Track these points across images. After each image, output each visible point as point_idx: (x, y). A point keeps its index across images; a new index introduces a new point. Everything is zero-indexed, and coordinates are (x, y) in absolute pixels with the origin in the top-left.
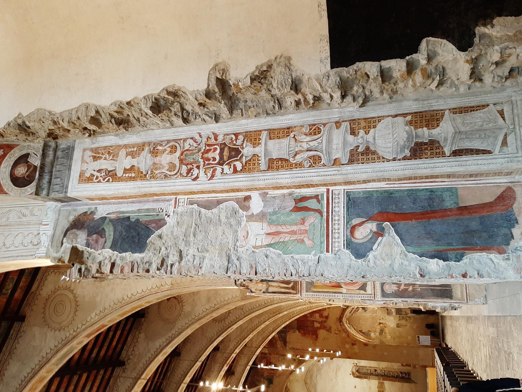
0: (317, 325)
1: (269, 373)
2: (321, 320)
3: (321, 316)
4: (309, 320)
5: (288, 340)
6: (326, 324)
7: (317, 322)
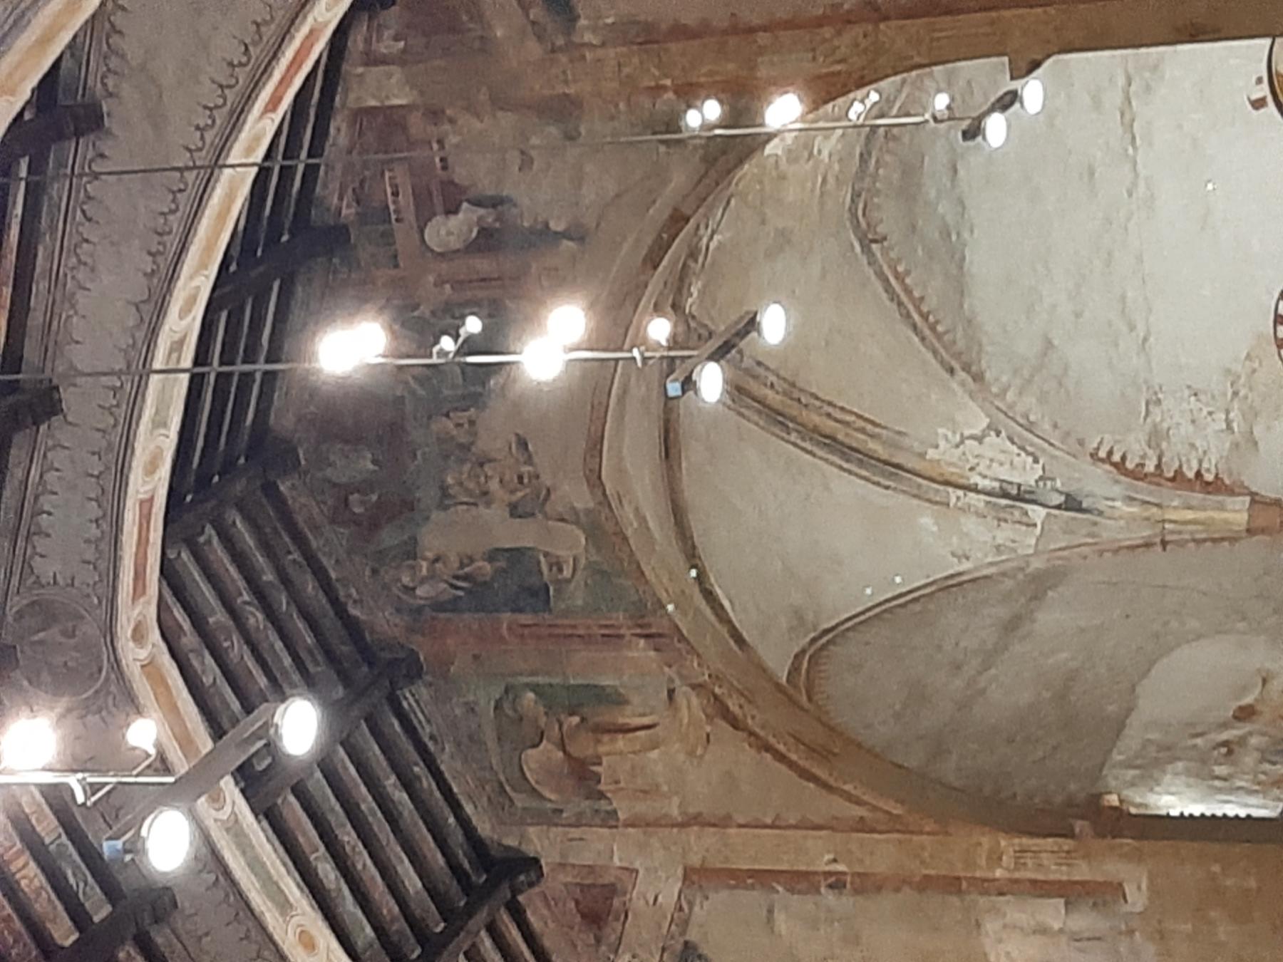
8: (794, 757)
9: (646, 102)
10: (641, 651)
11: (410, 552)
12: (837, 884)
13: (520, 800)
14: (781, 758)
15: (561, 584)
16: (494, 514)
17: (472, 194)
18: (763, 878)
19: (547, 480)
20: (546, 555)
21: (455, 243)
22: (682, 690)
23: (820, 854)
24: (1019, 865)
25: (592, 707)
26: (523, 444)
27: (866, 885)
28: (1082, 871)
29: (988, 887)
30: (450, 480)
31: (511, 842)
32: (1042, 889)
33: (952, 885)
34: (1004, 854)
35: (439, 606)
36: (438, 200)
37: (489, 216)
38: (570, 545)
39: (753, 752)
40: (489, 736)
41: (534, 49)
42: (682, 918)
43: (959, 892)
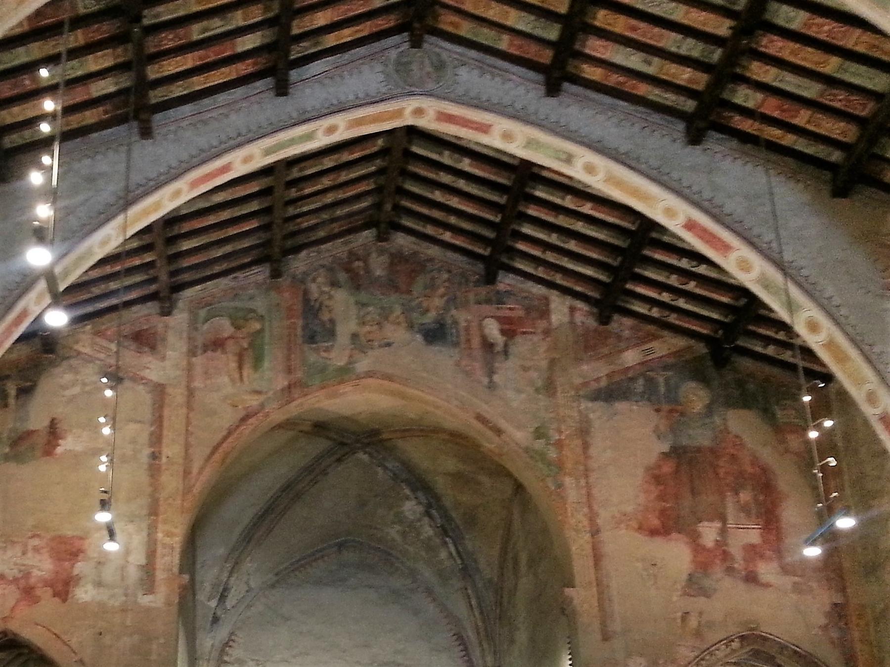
0: (709, 533)
1: (467, 329)
2: (735, 548)
3: (752, 551)
4: (723, 498)
6: (718, 571)
7: (723, 531)
8: (224, 445)
9: (554, 426)
10: (282, 382)
11: (334, 284)
12: (155, 456)
13: (203, 313)
14: (225, 438)
15: (317, 350)
16: (352, 326)
17: (510, 343)
18: (158, 420)
19: (370, 353)
20: (332, 346)
21: (487, 331)
22: (262, 398)
24: (164, 546)
25: (251, 354)
26: (389, 345)
28: (160, 575)
29: (152, 529)
30: (371, 309)
31: (180, 304)
32: (151, 554)
33: (154, 511)
35: (306, 293)
36: (507, 327)
37: (499, 348)
38: (338, 357)
39: (227, 426)
40: (238, 304)
41: (578, 381)
42: (137, 379)
43: (150, 514)
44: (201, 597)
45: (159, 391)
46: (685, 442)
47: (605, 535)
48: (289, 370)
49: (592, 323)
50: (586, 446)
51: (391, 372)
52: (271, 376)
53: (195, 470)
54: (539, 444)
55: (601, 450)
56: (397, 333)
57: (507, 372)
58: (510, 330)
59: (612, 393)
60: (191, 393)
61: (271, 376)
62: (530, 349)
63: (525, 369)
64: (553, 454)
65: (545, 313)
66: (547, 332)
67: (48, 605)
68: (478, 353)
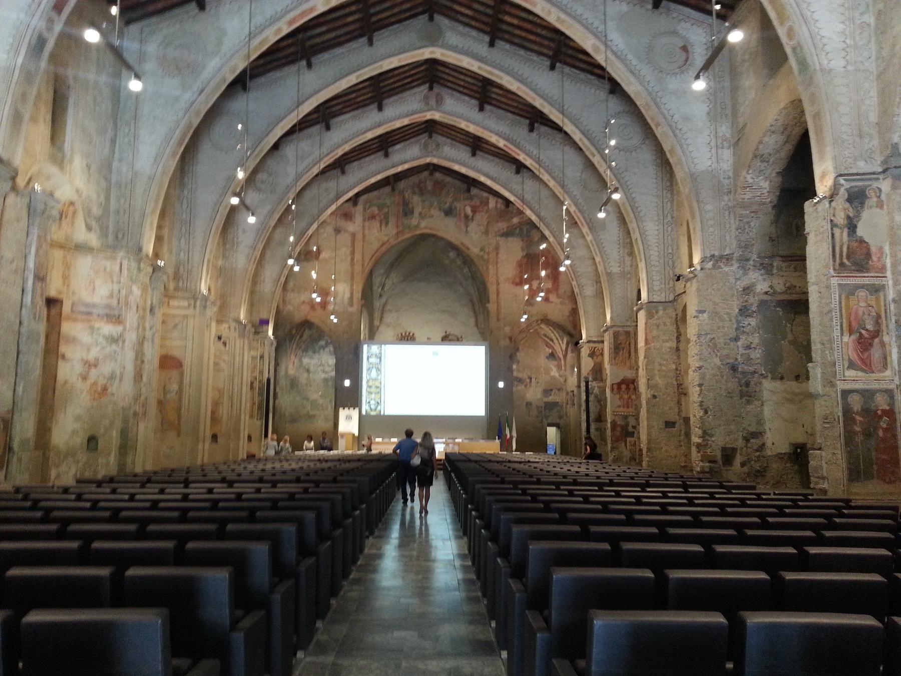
5: (510, 239)
10: (395, 231)
11: (414, 193)
12: (353, 259)
18: (353, 246)
23: (358, 257)
25: (385, 221)
27: (352, 263)
28: (355, 301)
29: (352, 286)
32: (352, 294)
34: (358, 289)
35: (404, 197)
41: (496, 229)
42: (346, 231)
44: (375, 288)
45: (353, 235)
46: (531, 252)
47: (501, 285)
48: (397, 227)
49: (503, 207)
50: (497, 254)
51: (433, 222)
52: (391, 230)
53: (366, 263)
54: (482, 253)
55: (503, 256)
56: (435, 212)
57: (473, 226)
58: (474, 211)
59: (507, 234)
60: (364, 236)
61: (392, 229)
62: (482, 218)
63: (479, 225)
64: (486, 257)
65: (487, 203)
66: (487, 211)
67: (319, 311)
68: (463, 219)
